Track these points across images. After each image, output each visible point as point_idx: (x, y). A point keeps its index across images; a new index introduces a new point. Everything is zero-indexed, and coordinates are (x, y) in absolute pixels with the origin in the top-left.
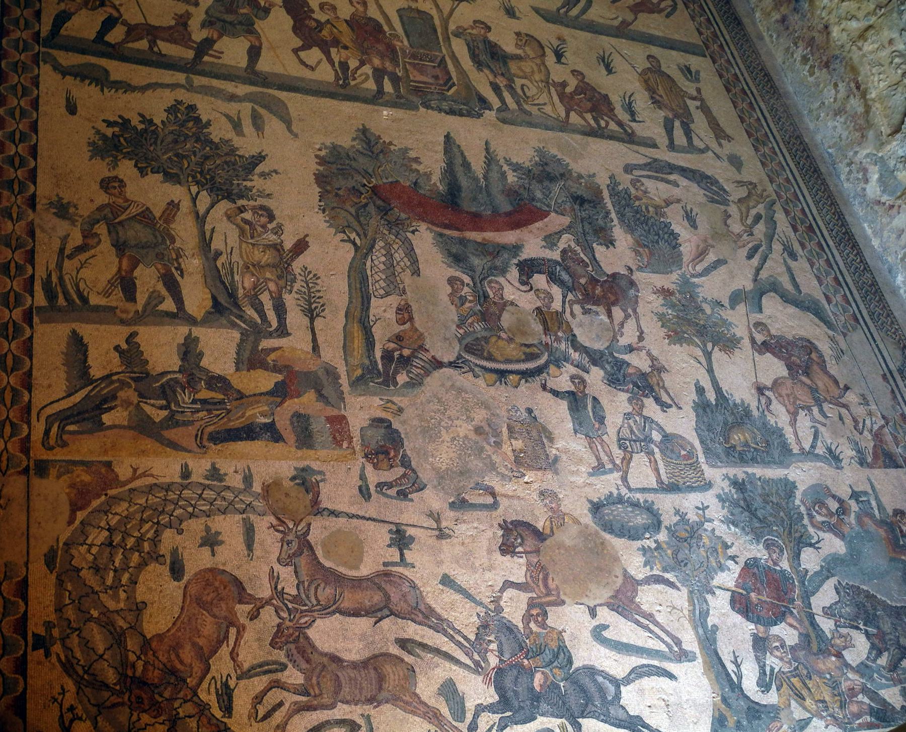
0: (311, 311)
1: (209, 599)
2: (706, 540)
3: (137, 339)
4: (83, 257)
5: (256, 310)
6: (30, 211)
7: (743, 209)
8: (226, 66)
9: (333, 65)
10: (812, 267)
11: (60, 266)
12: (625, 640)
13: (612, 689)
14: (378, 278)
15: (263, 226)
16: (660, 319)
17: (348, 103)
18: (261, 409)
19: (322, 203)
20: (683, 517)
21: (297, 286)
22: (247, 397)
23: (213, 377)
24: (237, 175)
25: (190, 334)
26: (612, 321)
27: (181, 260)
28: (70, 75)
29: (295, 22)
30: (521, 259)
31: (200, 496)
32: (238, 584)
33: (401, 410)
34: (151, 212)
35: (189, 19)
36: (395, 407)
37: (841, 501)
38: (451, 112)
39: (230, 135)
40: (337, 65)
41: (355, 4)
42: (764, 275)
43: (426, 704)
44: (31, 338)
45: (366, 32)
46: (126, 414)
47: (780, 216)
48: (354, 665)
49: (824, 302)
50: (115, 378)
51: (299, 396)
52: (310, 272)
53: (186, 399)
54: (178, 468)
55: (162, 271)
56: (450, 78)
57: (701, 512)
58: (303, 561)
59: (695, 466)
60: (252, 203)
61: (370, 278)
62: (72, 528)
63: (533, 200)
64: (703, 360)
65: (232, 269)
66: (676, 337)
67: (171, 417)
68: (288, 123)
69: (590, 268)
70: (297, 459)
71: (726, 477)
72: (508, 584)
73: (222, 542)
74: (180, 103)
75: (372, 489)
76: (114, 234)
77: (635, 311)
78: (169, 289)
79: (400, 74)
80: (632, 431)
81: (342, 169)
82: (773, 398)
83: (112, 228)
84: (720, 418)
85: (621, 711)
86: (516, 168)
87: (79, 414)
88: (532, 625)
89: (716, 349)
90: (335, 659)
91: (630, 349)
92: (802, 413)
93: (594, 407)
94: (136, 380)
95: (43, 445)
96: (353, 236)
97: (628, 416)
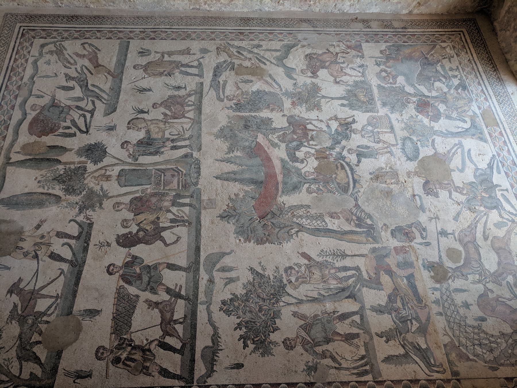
0: (342, 256)
1: (490, 307)
2: (412, 123)
3: (380, 333)
4: (339, 359)
5: (348, 280)
6: (316, 385)
7: (235, 57)
8: (186, 283)
9: (174, 227)
10: (264, 40)
11: (347, 369)
12: (461, 162)
13: (480, 171)
14: (316, 224)
15: (298, 272)
16: (309, 110)
17: (203, 222)
18: (400, 281)
19: (276, 243)
20: (405, 129)
21: (330, 260)
22: (396, 287)
23: (390, 300)
24: (267, 282)
25: (370, 309)
26: (316, 130)
27: (328, 312)
28: (212, 368)
29: (142, 243)
30: (289, 160)
31: (448, 309)
32: (481, 296)
33: (385, 225)
34: (302, 325)
35: (151, 301)
36: (384, 227)
37: (382, 71)
38: (199, 173)
39: (240, 284)
40: (174, 225)
41: (120, 208)
42: (273, 61)
43: (506, 234)
44: (392, 381)
45: (142, 206)
46: (419, 338)
47: (236, 43)
48: (499, 257)
49: (283, 42)
50: (402, 343)
51: (388, 265)
52: (320, 253)
53: (404, 312)
54: (439, 317)
55: (338, 321)
56: (172, 169)
57: (400, 122)
58: (465, 272)
59: (380, 117)
60: (284, 276)
61: (317, 227)
62: (478, 360)
63: (250, 147)
64: (328, 100)
65: (327, 288)
66: (318, 107)
67: (416, 321)
68: (224, 254)
69: (287, 132)
70: (420, 269)
71: (382, 108)
72: (450, 197)
73: (465, 301)
74: (221, 309)
75: (424, 241)
76: (321, 343)
77: (308, 120)
78: (348, 318)
79: (175, 194)
80: (370, 137)
81: (251, 231)
82: (340, 79)
83: (318, 344)
84: (355, 102)
85: (487, 170)
86: (231, 150)
87: (425, 358)
88: (465, 192)
89: (319, 92)
90: (499, 264)
91: (328, 126)
92: (344, 71)
93: (362, 148)
94: (401, 334)
95: (444, 373)
96: (293, 231)
97: (363, 136)
